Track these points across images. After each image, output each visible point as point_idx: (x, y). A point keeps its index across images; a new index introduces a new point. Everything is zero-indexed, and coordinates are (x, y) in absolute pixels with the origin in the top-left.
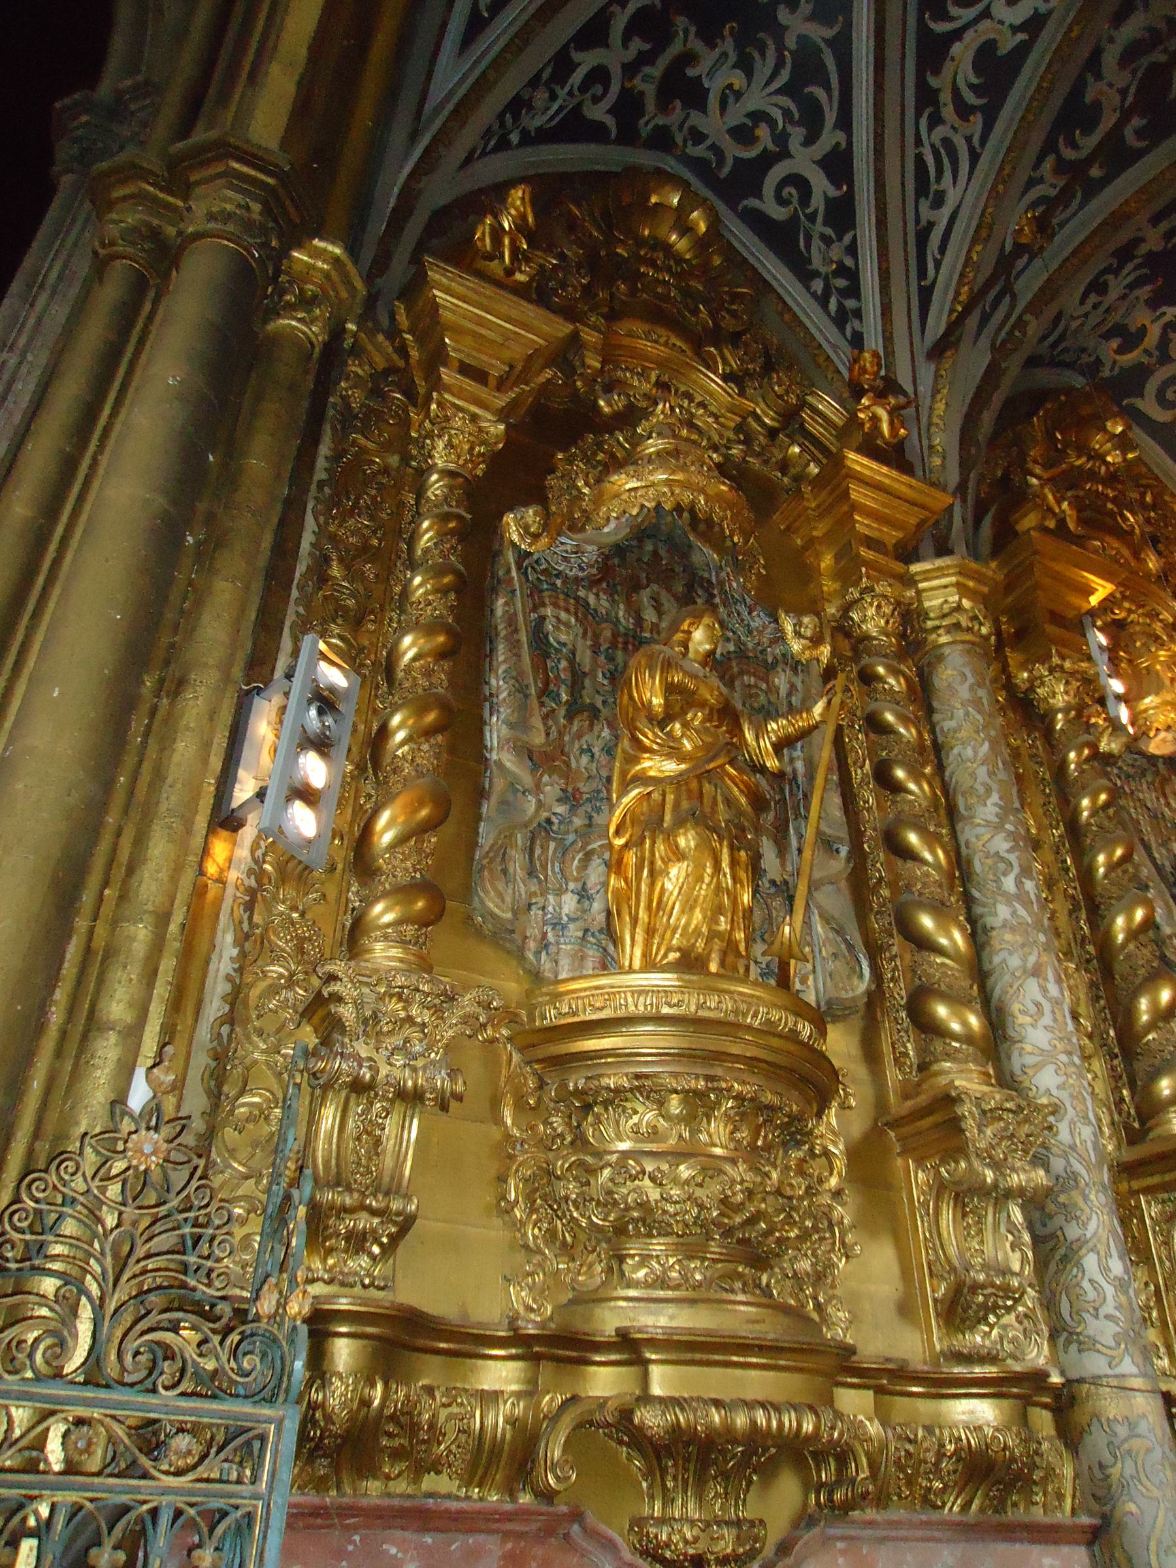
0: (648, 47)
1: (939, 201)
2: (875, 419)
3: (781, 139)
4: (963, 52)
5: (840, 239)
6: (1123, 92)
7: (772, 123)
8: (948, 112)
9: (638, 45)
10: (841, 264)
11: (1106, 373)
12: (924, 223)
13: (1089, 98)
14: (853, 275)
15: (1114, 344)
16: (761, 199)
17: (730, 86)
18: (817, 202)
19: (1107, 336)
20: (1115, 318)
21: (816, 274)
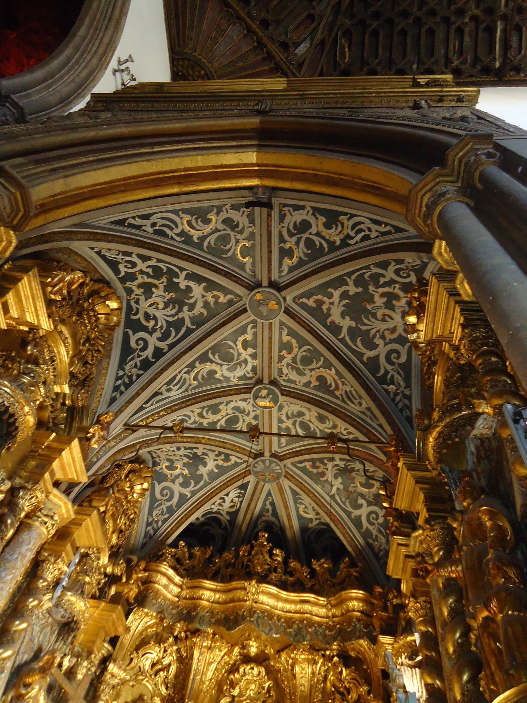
0: (152, 274)
1: (169, 390)
2: (93, 436)
3: (154, 330)
4: (209, 366)
5: (139, 370)
7: (156, 324)
8: (193, 374)
9: (150, 270)
10: (132, 375)
11: (158, 468)
12: (160, 391)
13: (221, 407)
14: (131, 383)
15: (167, 464)
16: (134, 334)
17: (158, 304)
18: (144, 354)
19: (168, 460)
20: (175, 458)
21: (124, 370)
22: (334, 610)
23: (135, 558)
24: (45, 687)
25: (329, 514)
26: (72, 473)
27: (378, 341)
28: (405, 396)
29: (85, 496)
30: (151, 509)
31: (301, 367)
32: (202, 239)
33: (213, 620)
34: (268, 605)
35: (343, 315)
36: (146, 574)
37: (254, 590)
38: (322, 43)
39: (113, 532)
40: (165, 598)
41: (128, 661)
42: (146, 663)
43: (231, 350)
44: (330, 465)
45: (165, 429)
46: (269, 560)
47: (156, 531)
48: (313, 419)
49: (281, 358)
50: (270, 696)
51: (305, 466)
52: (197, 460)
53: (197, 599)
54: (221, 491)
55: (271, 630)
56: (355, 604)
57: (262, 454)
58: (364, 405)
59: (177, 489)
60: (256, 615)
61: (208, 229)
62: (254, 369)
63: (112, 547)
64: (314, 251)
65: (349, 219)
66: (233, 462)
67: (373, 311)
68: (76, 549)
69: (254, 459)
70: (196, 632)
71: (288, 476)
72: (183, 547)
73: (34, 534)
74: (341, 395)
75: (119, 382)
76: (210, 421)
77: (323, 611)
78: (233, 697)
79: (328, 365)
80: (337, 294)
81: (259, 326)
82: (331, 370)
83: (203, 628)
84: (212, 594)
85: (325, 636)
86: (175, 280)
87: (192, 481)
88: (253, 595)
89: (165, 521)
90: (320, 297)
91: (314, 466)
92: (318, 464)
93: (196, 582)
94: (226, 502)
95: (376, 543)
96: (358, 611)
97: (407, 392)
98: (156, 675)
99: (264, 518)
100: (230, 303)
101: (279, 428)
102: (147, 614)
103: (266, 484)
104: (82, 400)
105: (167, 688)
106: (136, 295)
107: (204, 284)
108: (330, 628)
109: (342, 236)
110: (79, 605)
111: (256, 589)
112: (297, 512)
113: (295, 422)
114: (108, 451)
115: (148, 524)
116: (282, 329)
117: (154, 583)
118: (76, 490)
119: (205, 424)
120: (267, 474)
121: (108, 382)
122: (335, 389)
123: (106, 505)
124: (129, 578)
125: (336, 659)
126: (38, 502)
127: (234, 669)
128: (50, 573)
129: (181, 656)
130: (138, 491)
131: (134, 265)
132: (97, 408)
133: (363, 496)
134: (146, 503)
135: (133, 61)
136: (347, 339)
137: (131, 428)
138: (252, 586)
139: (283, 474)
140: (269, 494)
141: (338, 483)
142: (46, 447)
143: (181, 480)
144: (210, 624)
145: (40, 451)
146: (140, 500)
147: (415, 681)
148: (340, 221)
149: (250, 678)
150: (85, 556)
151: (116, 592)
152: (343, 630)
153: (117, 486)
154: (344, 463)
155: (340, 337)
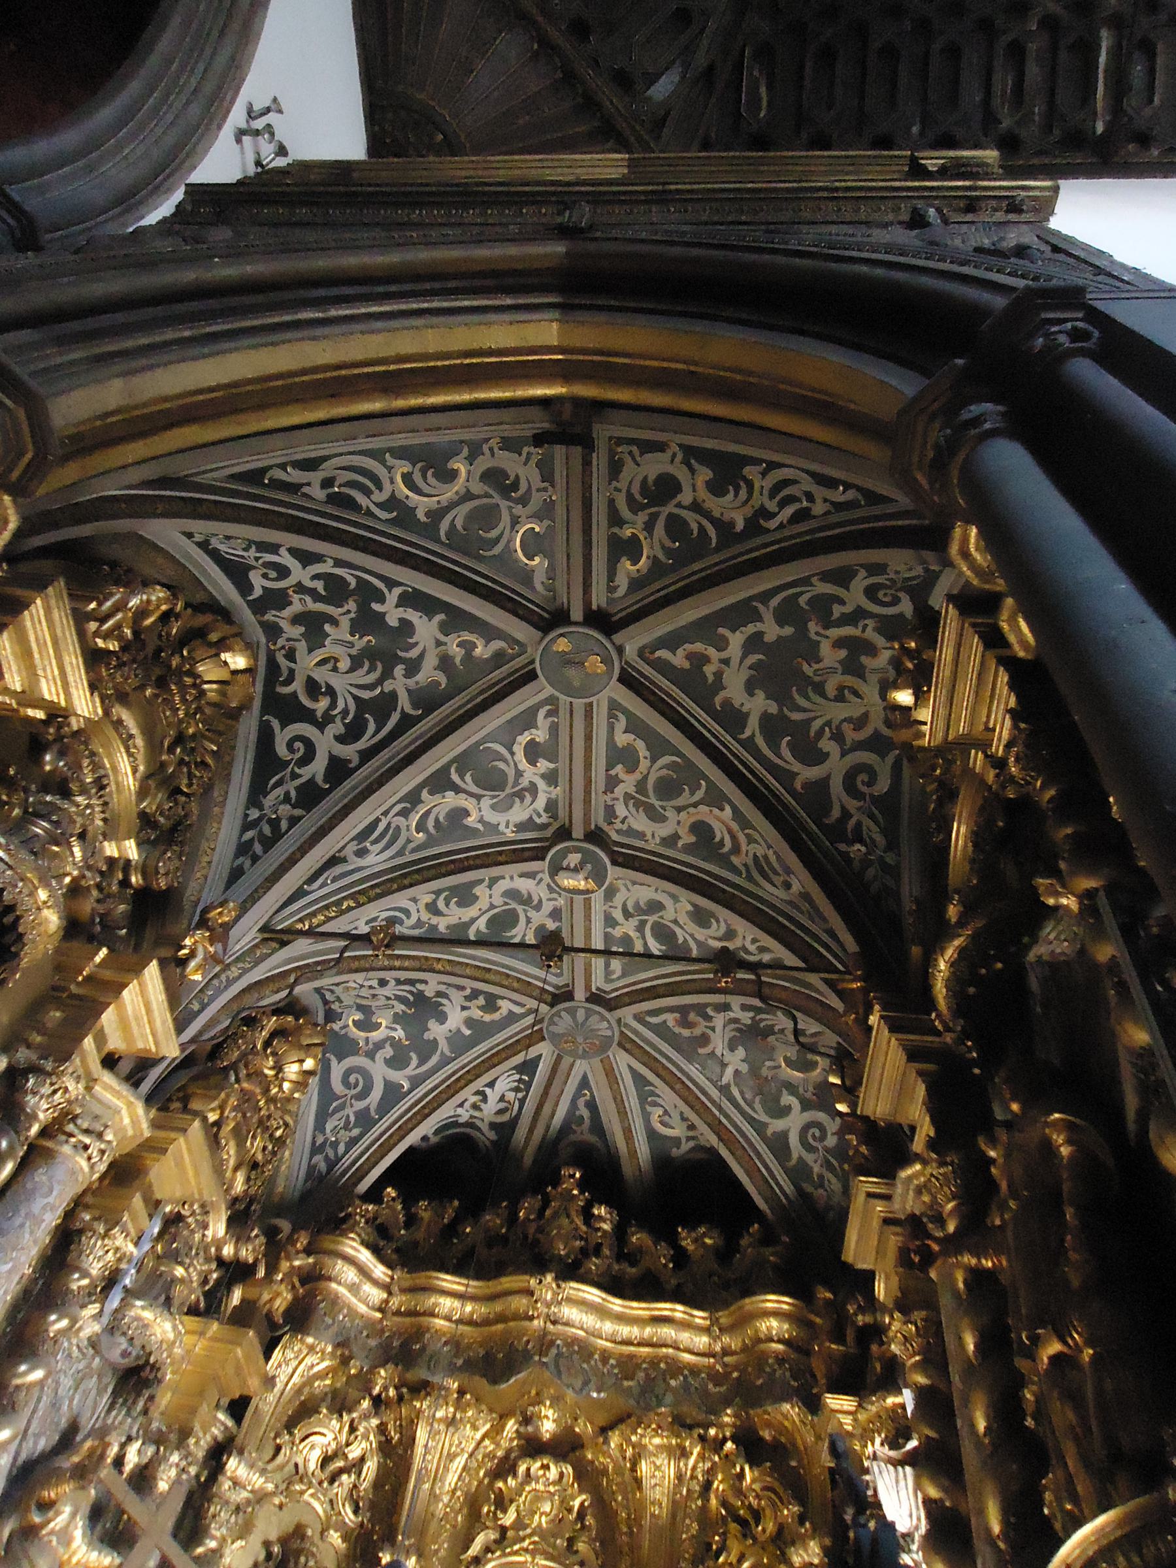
1: (362, 853)
2: (192, 954)
3: (328, 719)
4: (450, 800)
5: (294, 807)
6: (492, 907)
7: (333, 705)
8: (415, 818)
9: (319, 586)
10: (278, 819)
11: (336, 1026)
12: (342, 854)
13: (477, 891)
14: (277, 835)
17: (337, 660)
18: (306, 772)
19: (360, 1008)
20: (374, 1004)
21: (261, 807)
22: (726, 1339)
23: (285, 1226)
24: (85, 1509)
25: (717, 1127)
26: (144, 1036)
28: (885, 867)
29: (174, 1090)
30: (322, 1117)
31: (657, 803)
32: (436, 515)
33: (460, 1362)
34: (582, 1328)
35: (750, 687)
36: (311, 1260)
37: (549, 1297)
38: (710, 71)
39: (236, 1169)
40: (352, 1313)
41: (271, 1453)
42: (311, 1454)
43: (501, 765)
44: (719, 1020)
45: (354, 938)
46: (584, 1228)
47: (331, 1164)
48: (683, 919)
49: (612, 783)
50: (583, 1527)
52: (423, 1008)
53: (424, 1314)
54: (478, 1076)
55: (586, 1383)
56: (773, 1325)
57: (568, 996)
58: (796, 887)
59: (380, 1071)
60: (554, 1351)
61: (450, 492)
62: (551, 806)
63: (235, 1200)
64: (686, 543)
65: (764, 474)
66: (504, 1011)
67: (817, 679)
68: (154, 1205)
69: (552, 1005)
70: (421, 1388)
71: (626, 1044)
72: (393, 1199)
73: (59, 1172)
74: (745, 865)
75: (249, 834)
76: (453, 920)
77: (702, 1341)
78: (503, 1530)
79: (716, 799)
80: (736, 640)
81: (563, 712)
82: (722, 809)
83: (435, 1379)
84: (457, 1304)
85: (706, 1393)
86: (376, 607)
87: (413, 1055)
88: (548, 1306)
89: (353, 1142)
90: (698, 647)
91: (685, 1023)
92: (692, 1016)
93: (421, 1278)
94: (490, 1100)
95: (821, 1191)
96: (779, 1341)
97: (890, 859)
98: (332, 1479)
99: (572, 1137)
100: (499, 659)
101: (607, 936)
102: (311, 1349)
103: (578, 1062)
104: (166, 874)
105: (356, 1512)
106: (289, 640)
107: (441, 617)
109: (748, 511)
110: (161, 1328)
111: (556, 1294)
112: (646, 1123)
113: (643, 923)
114: (226, 988)
115: (316, 1149)
116: (616, 718)
117: (330, 1279)
118: (155, 1074)
119: (442, 928)
120: (580, 1039)
121: (223, 834)
123: (222, 1108)
124: (272, 1269)
125: (729, 1445)
126: (69, 1102)
127: (505, 1467)
128: (96, 1259)
129: (389, 1441)
130: (293, 1077)
131: (283, 572)
132: (201, 891)
133: (791, 1088)
134: (310, 1101)
135: (280, 111)
136: (760, 741)
137: (275, 937)
138: (546, 1286)
139: (616, 1038)
140: (584, 1083)
141: (736, 1060)
142: (88, 979)
143: (388, 1052)
144: (452, 1370)
145: (72, 987)
146: (296, 1095)
147: (903, 1493)
148: (745, 479)
149: (540, 1487)
150: (174, 1221)
151: (243, 1300)
152: (746, 1383)
153: (246, 1066)
154: (751, 1014)
155: (743, 736)
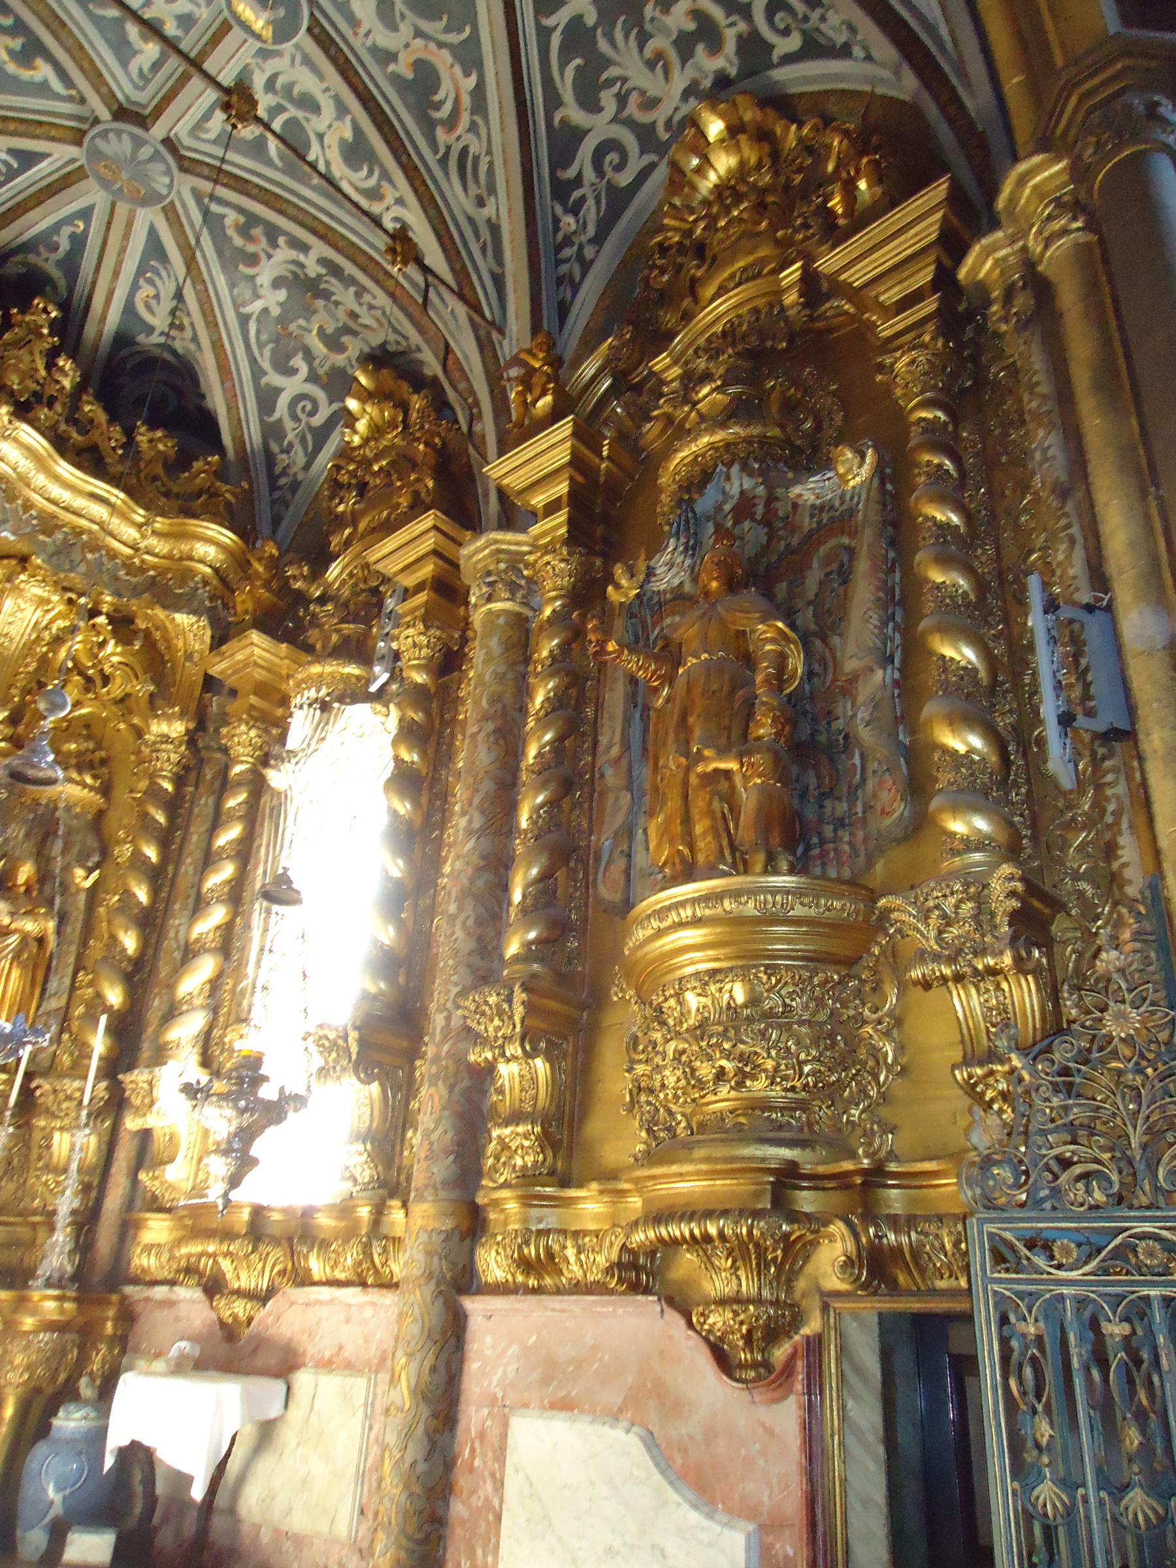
22: (153, 541)
25: (217, 346)
27: (607, 98)
44: (283, 254)
46: (43, 373)
51: (224, 216)
56: (203, 550)
58: (489, 211)
71: (171, 213)
74: (448, 148)
77: (131, 533)
82: (467, 74)
85: (117, 579)
92: (257, 232)
97: (589, 252)
99: (32, 258)
108: (129, 567)
120: (124, 176)
122: (441, 122)
133: (309, 355)
136: (556, 40)
140: (86, 214)
141: (273, 300)
152: (166, 586)
154: (323, 271)
